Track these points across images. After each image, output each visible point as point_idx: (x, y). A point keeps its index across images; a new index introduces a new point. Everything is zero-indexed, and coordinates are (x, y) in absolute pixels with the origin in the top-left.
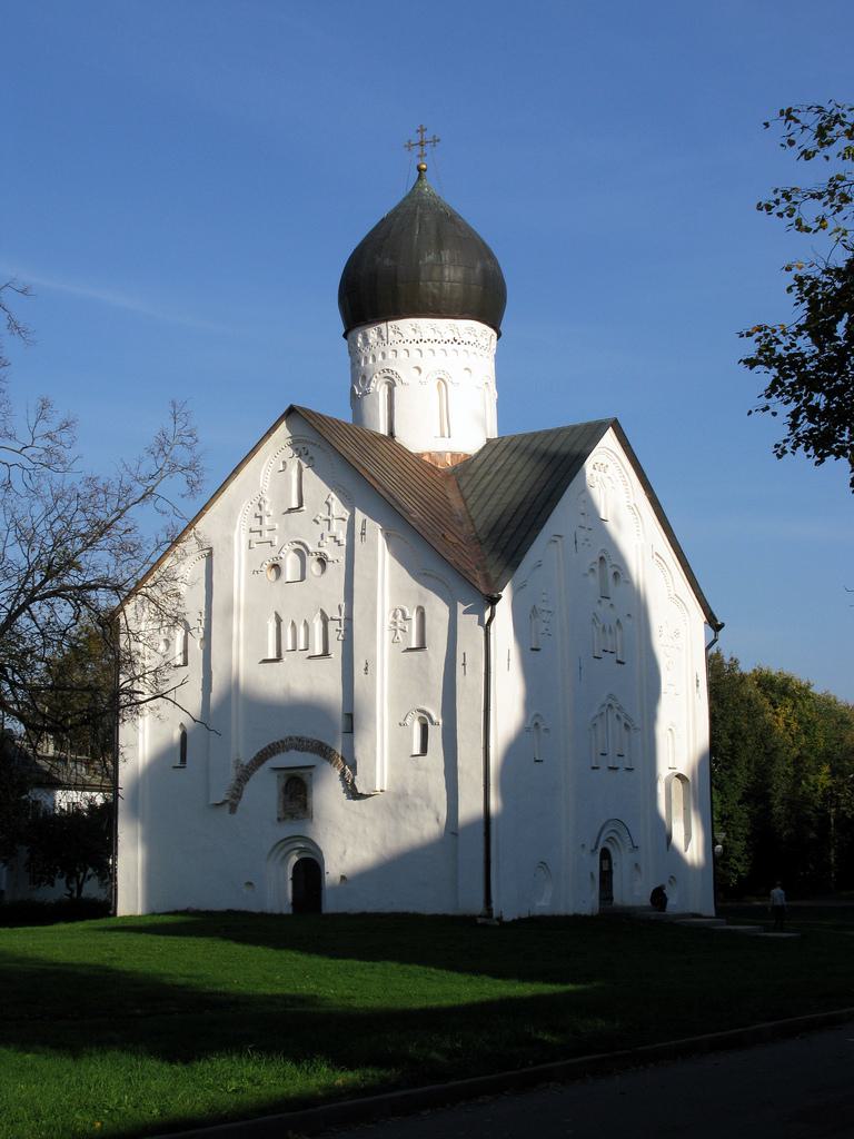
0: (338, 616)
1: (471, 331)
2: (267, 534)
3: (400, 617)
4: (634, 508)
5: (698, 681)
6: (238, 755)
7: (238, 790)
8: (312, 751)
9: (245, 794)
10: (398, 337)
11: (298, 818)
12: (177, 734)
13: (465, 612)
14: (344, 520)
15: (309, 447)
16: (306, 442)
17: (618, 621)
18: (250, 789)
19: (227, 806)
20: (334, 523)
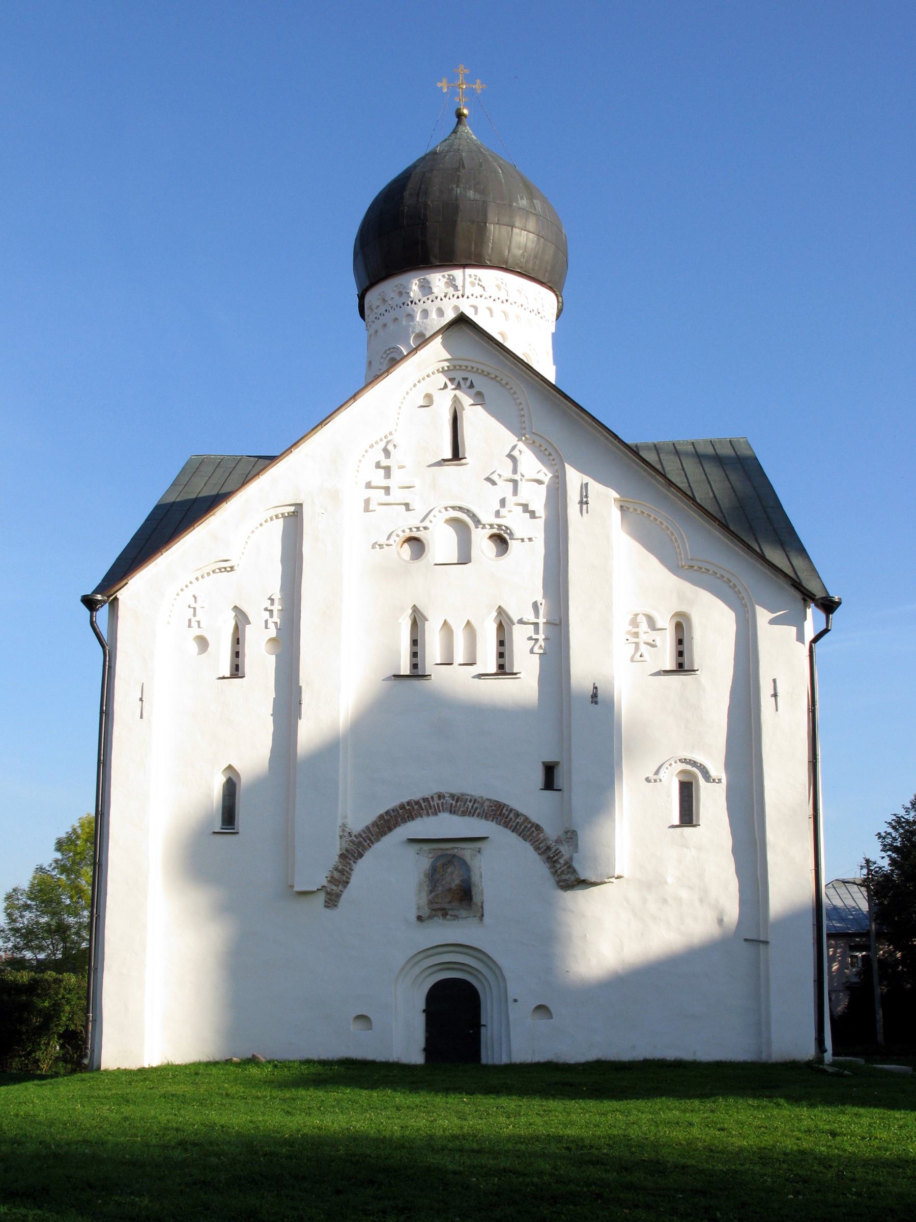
0: (530, 616)
2: (397, 495)
3: (644, 626)
6: (345, 817)
7: (342, 872)
8: (485, 816)
9: (355, 879)
10: (478, 290)
11: (456, 917)
12: (218, 783)
13: (773, 622)
14: (540, 482)
15: (478, 380)
16: (471, 370)
18: (362, 869)
19: (322, 897)
20: (523, 486)
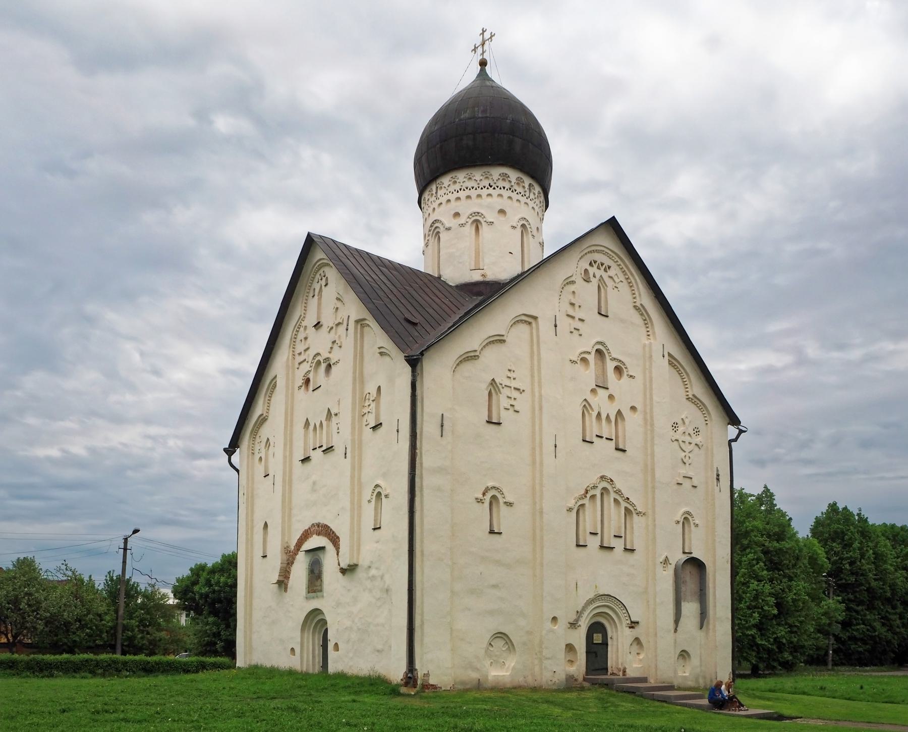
1: (505, 177)
4: (640, 309)
5: (718, 475)
17: (619, 413)
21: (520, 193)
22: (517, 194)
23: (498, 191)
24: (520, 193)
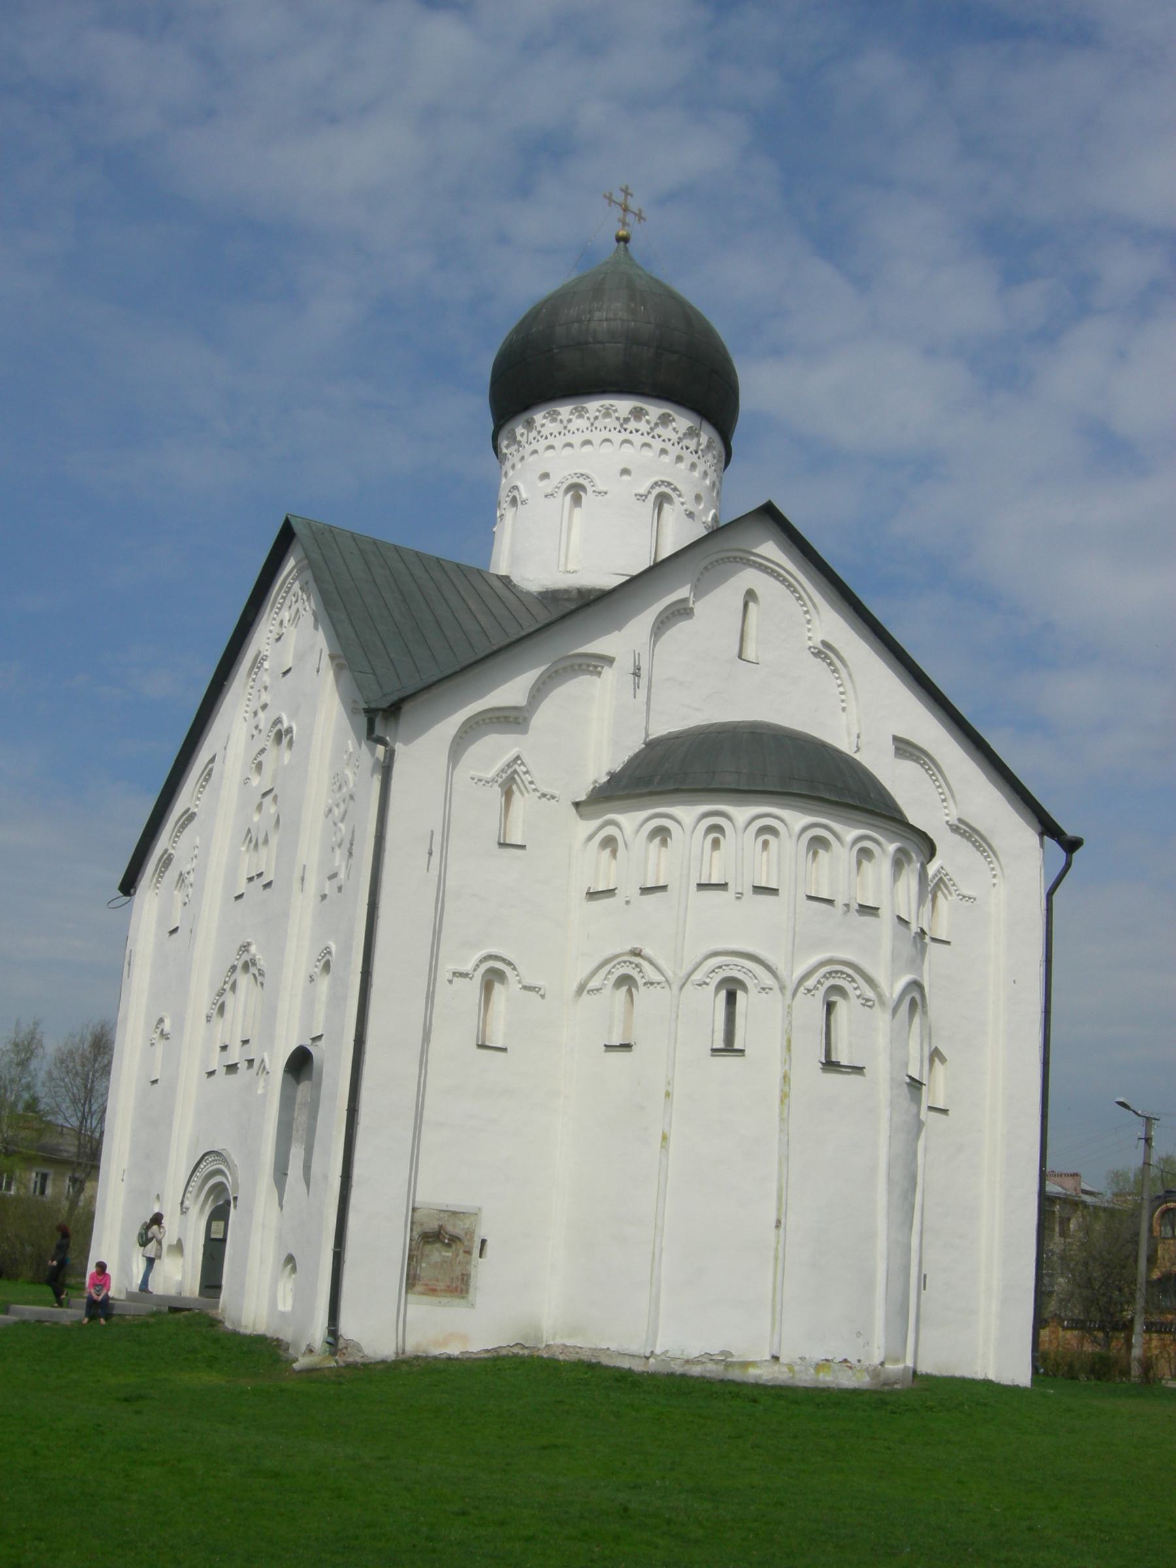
1: (638, 414)
21: (669, 440)
22: (664, 441)
23: (625, 435)
24: (669, 440)
